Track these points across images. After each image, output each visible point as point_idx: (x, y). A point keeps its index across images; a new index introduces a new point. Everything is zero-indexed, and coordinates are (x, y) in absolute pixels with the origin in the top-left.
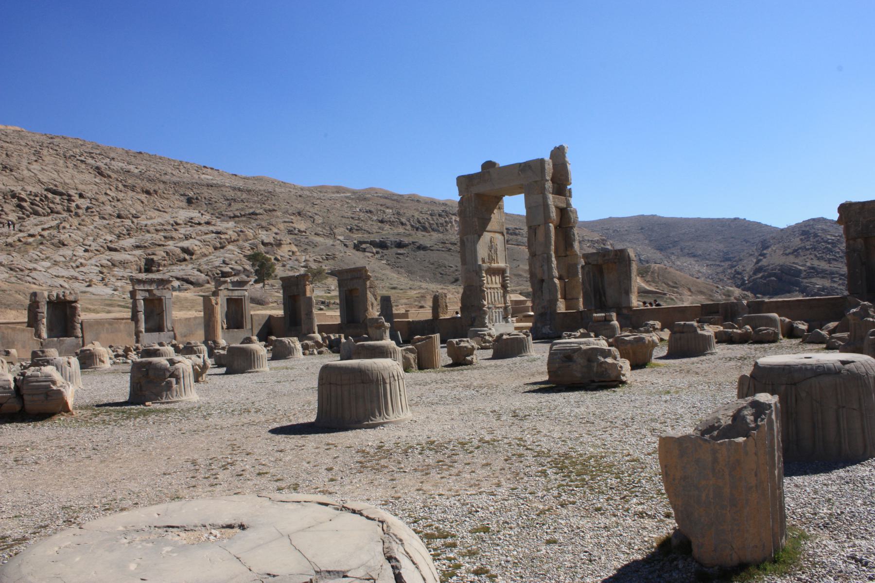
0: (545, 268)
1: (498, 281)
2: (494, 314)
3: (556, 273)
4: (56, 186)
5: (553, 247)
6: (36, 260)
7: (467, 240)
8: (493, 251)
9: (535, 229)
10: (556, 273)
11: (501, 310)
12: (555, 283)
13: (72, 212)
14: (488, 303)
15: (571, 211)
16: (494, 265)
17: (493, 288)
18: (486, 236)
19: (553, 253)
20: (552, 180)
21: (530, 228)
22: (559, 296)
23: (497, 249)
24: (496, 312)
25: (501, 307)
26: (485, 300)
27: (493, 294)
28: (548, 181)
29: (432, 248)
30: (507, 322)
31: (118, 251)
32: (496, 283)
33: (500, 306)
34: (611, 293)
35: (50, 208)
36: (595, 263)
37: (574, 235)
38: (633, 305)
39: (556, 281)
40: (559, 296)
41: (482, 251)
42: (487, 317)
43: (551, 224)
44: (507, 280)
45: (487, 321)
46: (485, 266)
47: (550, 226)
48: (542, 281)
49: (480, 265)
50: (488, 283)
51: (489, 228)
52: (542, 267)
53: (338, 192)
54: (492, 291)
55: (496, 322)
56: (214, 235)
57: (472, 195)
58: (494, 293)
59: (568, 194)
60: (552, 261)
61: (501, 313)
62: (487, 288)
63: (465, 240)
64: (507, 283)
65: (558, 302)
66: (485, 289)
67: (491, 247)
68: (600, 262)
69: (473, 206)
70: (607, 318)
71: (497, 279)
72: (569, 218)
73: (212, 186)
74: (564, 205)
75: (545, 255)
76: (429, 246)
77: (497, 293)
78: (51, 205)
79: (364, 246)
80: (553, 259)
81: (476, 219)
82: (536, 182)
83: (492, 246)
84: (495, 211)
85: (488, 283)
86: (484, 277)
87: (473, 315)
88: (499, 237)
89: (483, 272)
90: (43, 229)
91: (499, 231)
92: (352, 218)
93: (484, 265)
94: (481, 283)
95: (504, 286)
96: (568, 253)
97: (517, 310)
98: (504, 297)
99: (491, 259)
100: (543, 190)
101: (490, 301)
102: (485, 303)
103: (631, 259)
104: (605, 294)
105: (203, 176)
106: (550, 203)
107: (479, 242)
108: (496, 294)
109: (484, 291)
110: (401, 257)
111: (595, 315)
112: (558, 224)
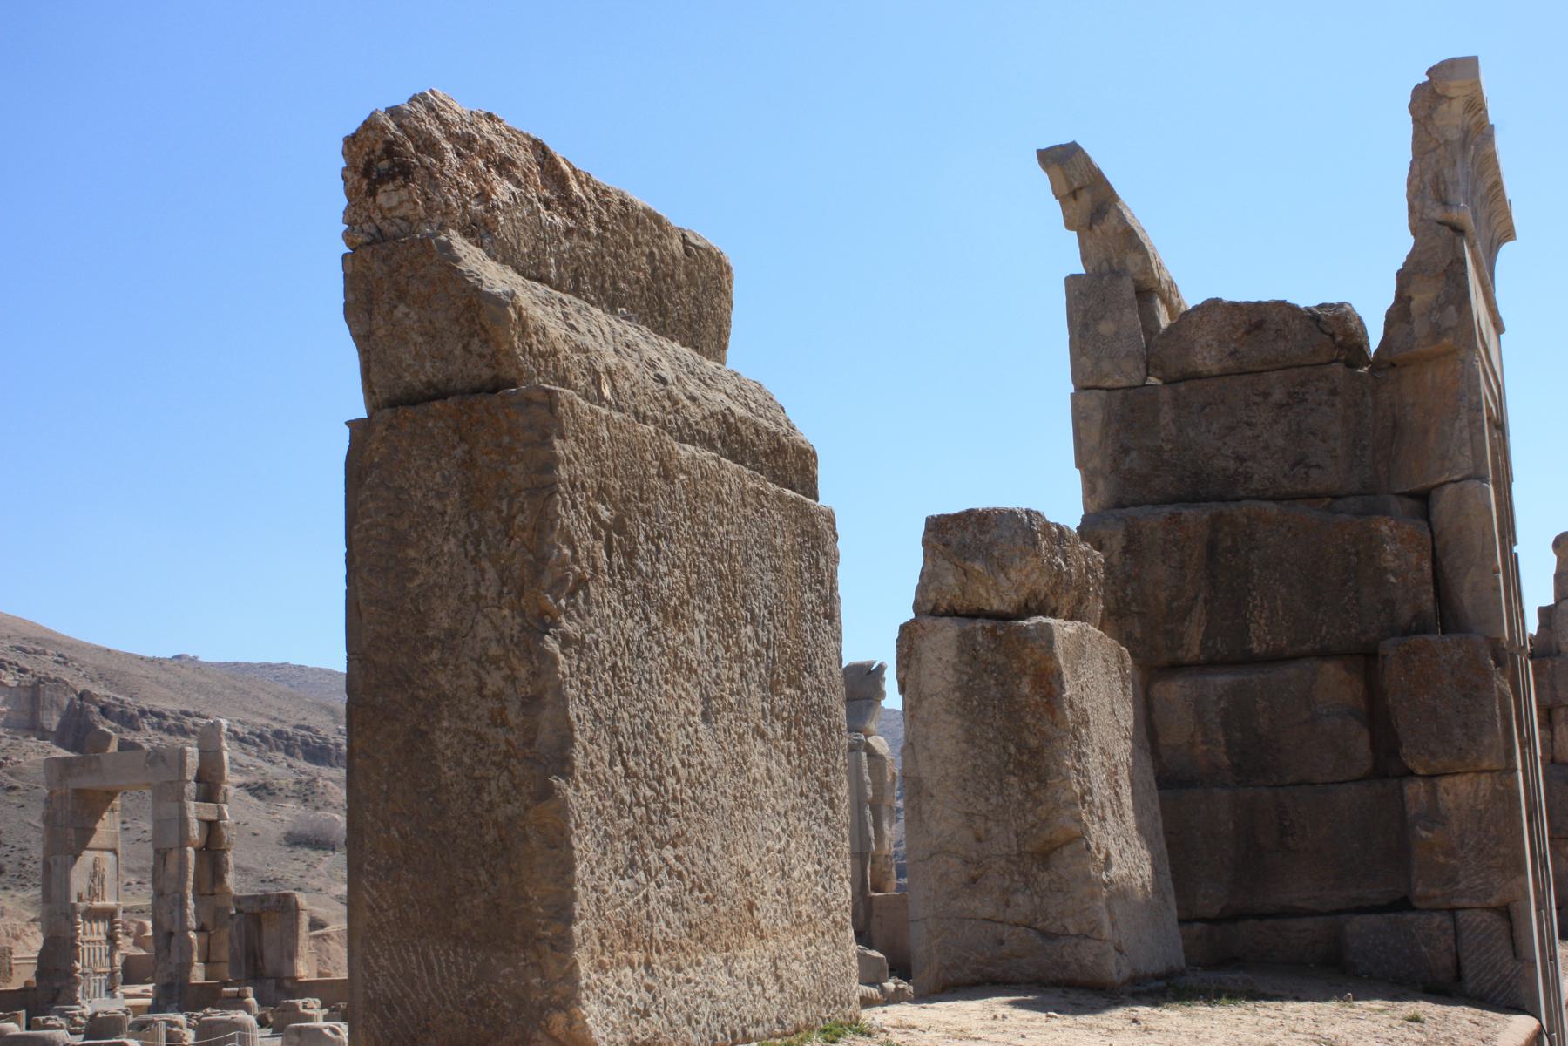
0: (176, 914)
1: (101, 930)
2: (92, 985)
3: (192, 922)
5: (190, 884)
7: (56, 863)
8: (96, 882)
9: (165, 854)
10: (192, 922)
11: (104, 977)
12: (190, 939)
14: (83, 966)
15: (225, 826)
16: (97, 904)
17: (94, 942)
18: (88, 857)
19: (190, 895)
20: (198, 780)
21: (157, 851)
22: (195, 958)
23: (103, 877)
24: (95, 980)
25: (105, 973)
26: (78, 962)
27: (92, 951)
28: (189, 781)
30: (113, 996)
32: (99, 933)
33: (102, 970)
34: (270, 954)
36: (250, 910)
37: (227, 863)
38: (299, 975)
39: (192, 935)
40: (195, 958)
41: (79, 880)
42: (80, 988)
43: (190, 849)
44: (118, 928)
45: (79, 995)
46: (82, 905)
47: (187, 851)
48: (171, 934)
49: (74, 905)
50: (85, 933)
51: (93, 843)
52: (171, 913)
54: (91, 946)
55: (95, 997)
57: (69, 791)
58: (94, 949)
59: (222, 799)
60: (187, 904)
61: (103, 982)
62: (82, 942)
63: (52, 862)
64: (118, 933)
65: (193, 968)
66: (80, 943)
67: (96, 873)
68: (256, 910)
69: (69, 808)
70: (241, 994)
71: (102, 927)
72: (221, 837)
74: (214, 817)
75: (177, 895)
77: (100, 949)
80: (190, 902)
81: (73, 831)
82: (171, 782)
83: (95, 873)
84: (105, 815)
85: (85, 933)
86: (79, 924)
87: (57, 985)
88: (110, 856)
89: (79, 915)
91: (110, 847)
93: (81, 904)
94: (74, 934)
95: (112, 939)
96: (216, 890)
97: (132, 973)
98: (111, 955)
99: (93, 894)
100: (180, 797)
101: (86, 964)
102: (79, 965)
103: (301, 907)
104: (262, 957)
106: (190, 816)
107: (74, 867)
108: (98, 951)
109: (78, 946)
111: (225, 989)
112: (203, 845)
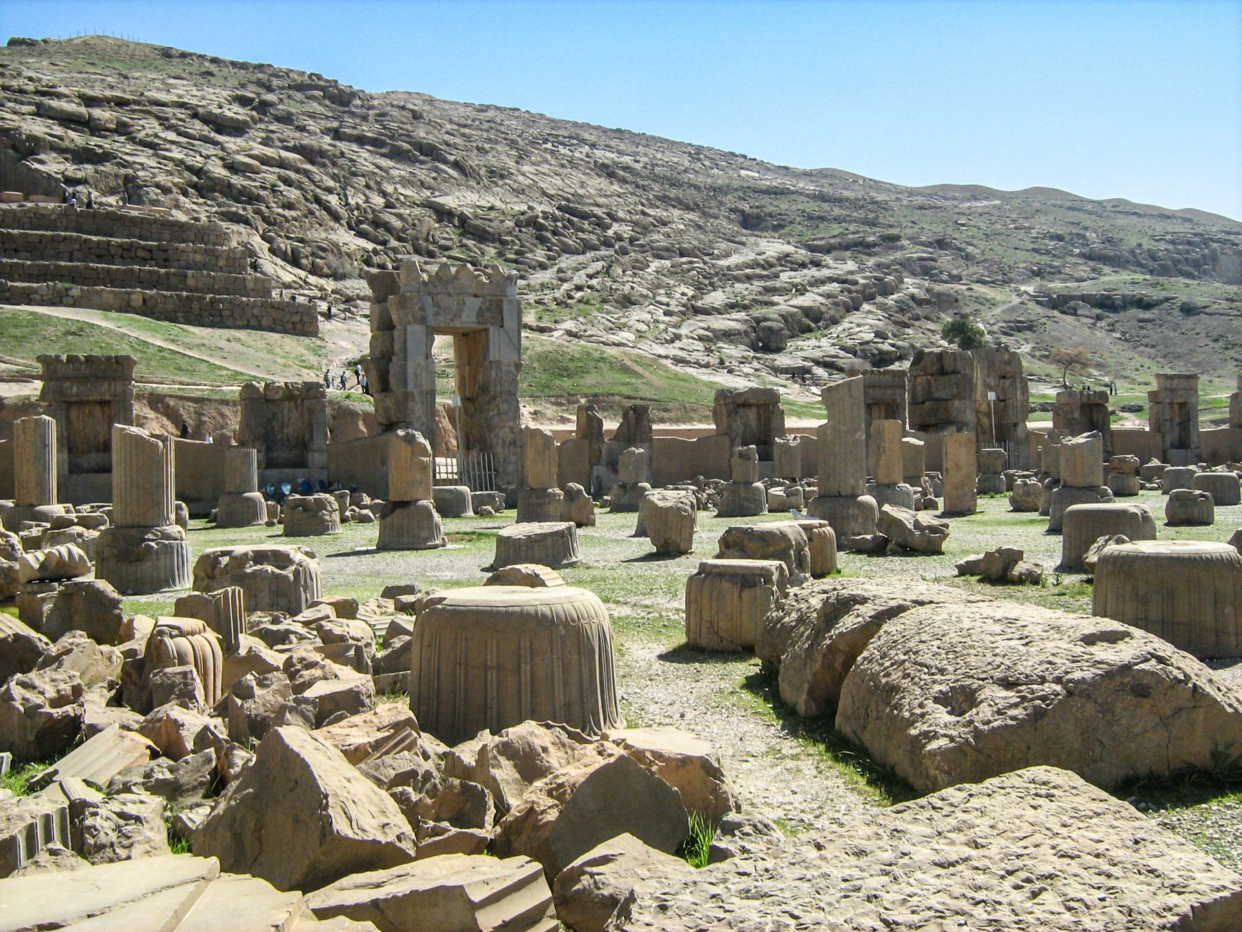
4: (568, 200)
6: (611, 329)
13: (612, 246)
29: (1207, 310)
31: (709, 314)
35: (582, 240)
53: (975, 198)
56: (835, 284)
73: (775, 193)
76: (1199, 304)
78: (581, 235)
79: (1072, 303)
90: (590, 277)
92: (1035, 250)
105: (743, 173)
110: (1149, 325)
